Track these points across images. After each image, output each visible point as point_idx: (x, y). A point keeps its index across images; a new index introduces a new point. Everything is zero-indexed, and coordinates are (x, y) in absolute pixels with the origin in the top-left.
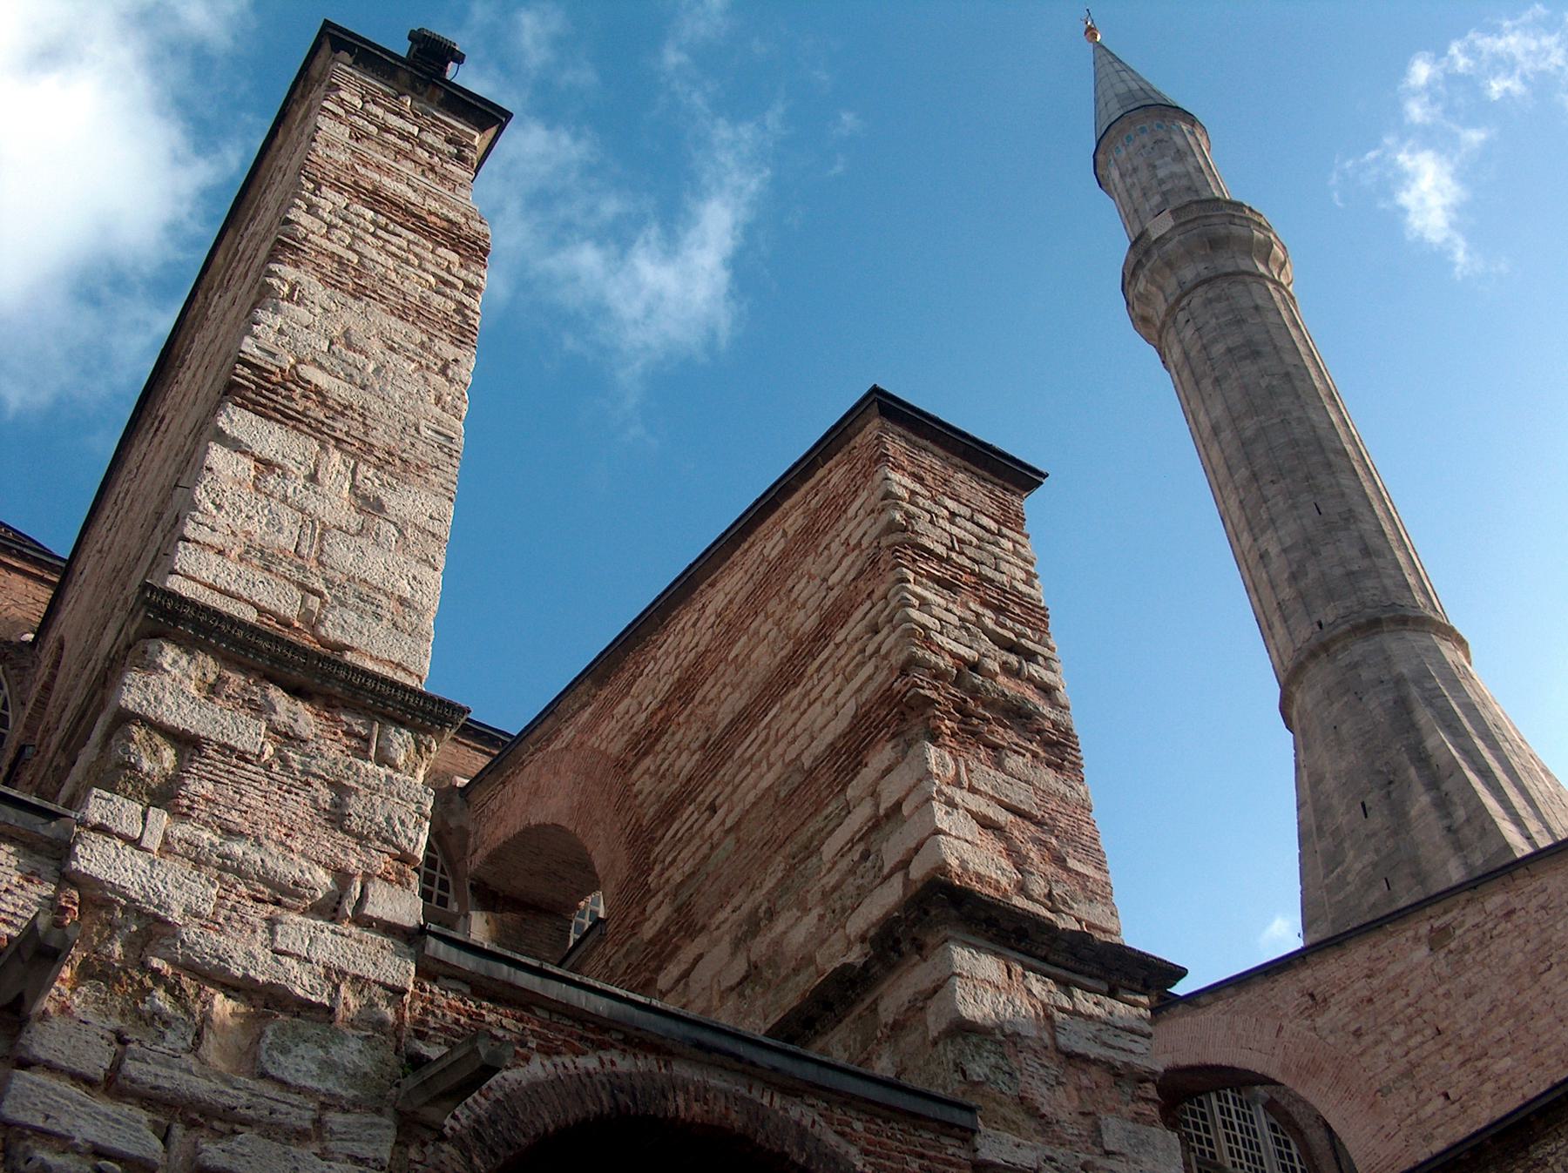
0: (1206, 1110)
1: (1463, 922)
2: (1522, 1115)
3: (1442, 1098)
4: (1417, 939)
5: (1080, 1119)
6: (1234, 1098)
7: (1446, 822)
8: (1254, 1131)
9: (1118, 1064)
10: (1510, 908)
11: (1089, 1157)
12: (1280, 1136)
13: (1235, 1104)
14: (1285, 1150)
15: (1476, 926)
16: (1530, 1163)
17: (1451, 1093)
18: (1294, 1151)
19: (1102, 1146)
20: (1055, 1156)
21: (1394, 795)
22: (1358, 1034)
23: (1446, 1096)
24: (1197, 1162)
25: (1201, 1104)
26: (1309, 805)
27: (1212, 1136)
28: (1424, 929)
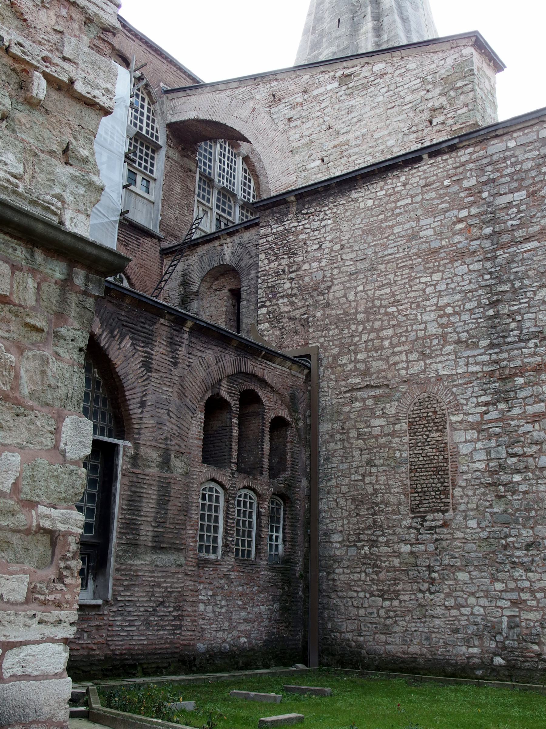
0: (213, 151)
1: (360, 74)
2: (353, 175)
3: (320, 161)
4: (334, 77)
5: (53, 32)
6: (229, 150)
7: (376, 39)
8: (235, 169)
9: (90, 12)
10: (386, 72)
11: (49, 55)
12: (247, 175)
13: (229, 153)
14: (247, 183)
15: (366, 77)
16: (350, 199)
17: (325, 160)
18: (252, 185)
19: (62, 53)
20: (24, 44)
21: (355, 19)
22: (290, 120)
23: (323, 161)
24: (200, 174)
25: (211, 147)
26: (313, 16)
27: (212, 165)
28: (339, 73)
